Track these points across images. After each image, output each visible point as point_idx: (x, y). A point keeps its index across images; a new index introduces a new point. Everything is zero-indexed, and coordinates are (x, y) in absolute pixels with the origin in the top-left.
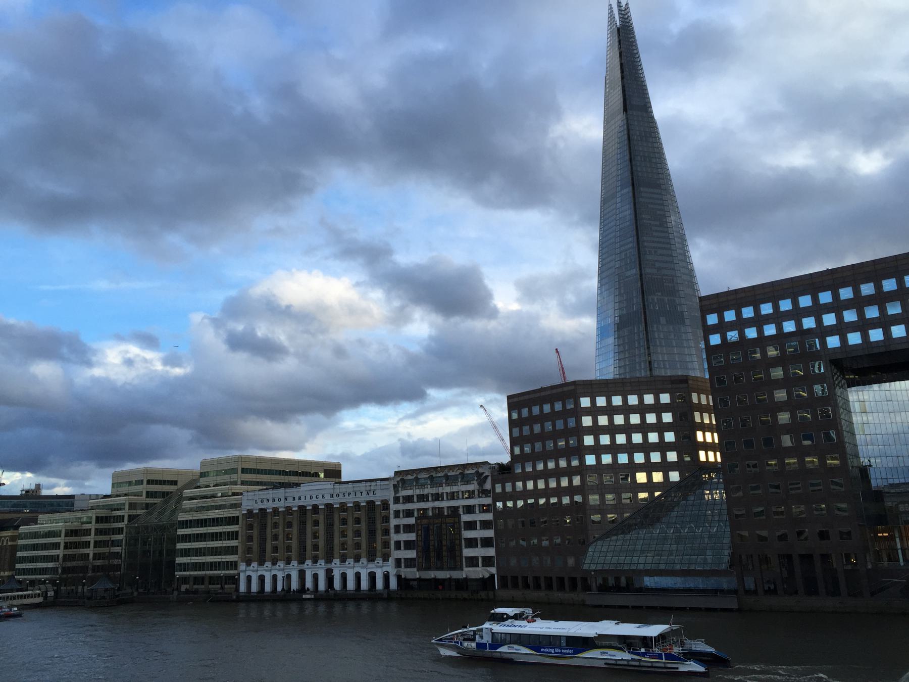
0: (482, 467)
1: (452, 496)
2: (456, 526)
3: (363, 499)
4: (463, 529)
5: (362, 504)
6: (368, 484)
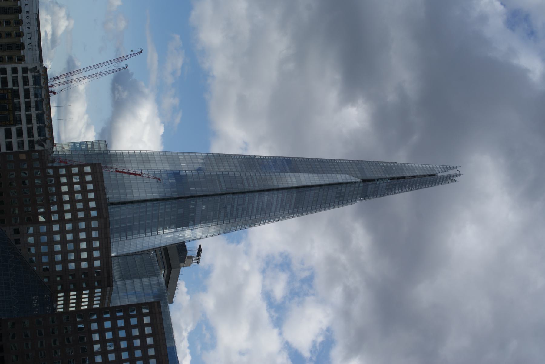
0: (50, 142)
1: (29, 120)
2: (8, 122)
3: (25, 40)
4: (5, 128)
5: (21, 39)
6: (37, 44)
